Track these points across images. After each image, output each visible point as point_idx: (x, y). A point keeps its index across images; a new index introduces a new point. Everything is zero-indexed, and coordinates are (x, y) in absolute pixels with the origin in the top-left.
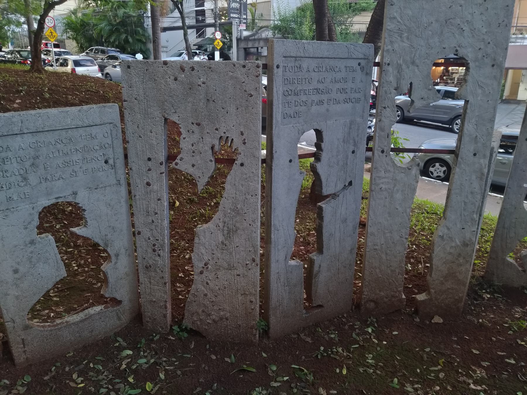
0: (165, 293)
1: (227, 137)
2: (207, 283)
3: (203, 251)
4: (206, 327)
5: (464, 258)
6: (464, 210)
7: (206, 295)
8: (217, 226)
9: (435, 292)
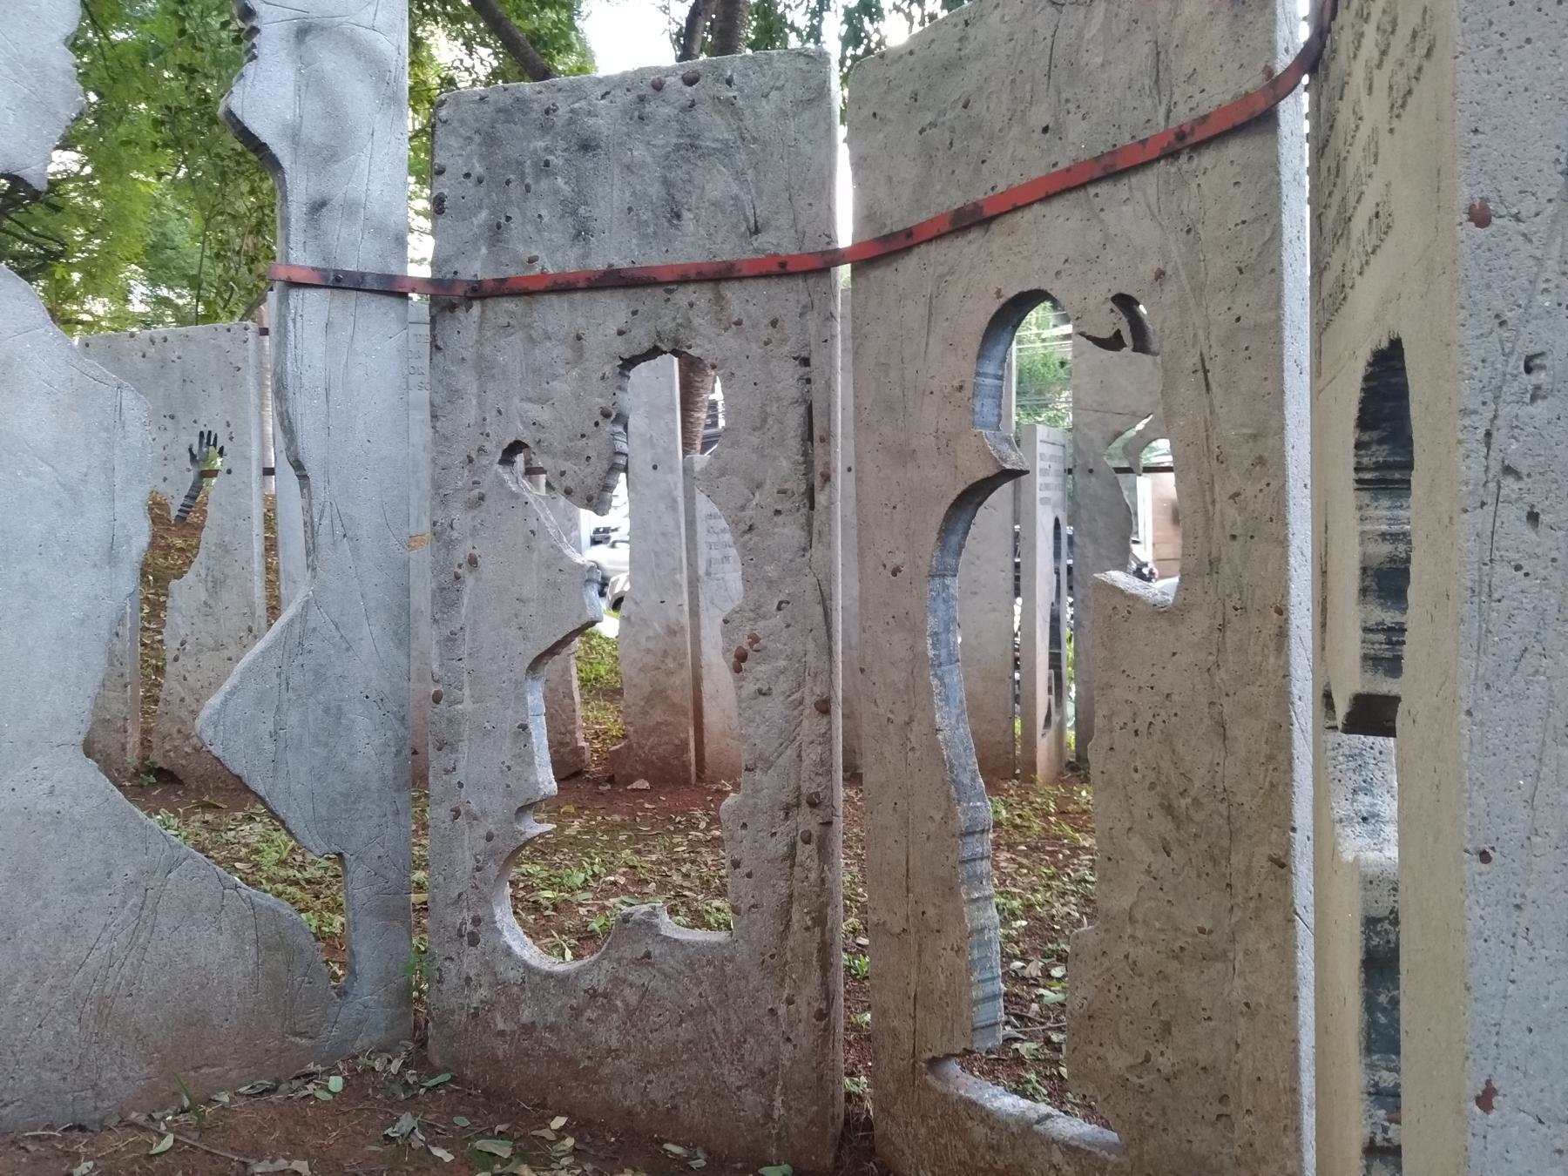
0: (125, 703)
1: (210, 432)
2: (185, 679)
3: (179, 619)
4: (184, 762)
5: (674, 659)
6: (657, 566)
7: (182, 700)
8: (198, 575)
9: (635, 731)
